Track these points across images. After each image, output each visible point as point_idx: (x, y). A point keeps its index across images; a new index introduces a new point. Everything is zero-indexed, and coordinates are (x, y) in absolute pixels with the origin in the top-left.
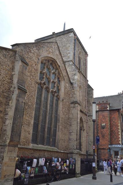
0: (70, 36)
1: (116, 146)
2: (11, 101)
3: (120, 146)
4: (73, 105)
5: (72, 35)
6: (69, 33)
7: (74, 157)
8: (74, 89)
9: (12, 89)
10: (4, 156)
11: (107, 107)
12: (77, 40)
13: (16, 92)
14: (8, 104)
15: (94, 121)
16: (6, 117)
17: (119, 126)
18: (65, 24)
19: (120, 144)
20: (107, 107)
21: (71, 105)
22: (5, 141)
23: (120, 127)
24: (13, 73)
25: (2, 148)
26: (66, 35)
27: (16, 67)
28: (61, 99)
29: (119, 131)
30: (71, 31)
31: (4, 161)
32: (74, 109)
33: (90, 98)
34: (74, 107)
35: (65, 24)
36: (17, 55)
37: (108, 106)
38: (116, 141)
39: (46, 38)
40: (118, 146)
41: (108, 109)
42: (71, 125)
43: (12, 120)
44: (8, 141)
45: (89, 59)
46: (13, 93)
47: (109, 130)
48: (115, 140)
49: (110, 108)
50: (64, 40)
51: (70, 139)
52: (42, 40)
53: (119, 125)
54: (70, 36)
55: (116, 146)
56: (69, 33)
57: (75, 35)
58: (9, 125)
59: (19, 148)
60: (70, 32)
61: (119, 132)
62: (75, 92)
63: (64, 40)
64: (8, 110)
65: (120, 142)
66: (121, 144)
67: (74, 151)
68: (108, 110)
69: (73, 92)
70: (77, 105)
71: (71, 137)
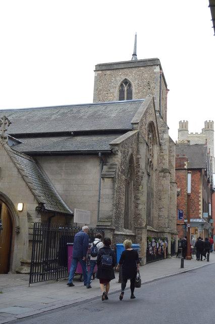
0: (155, 71)
1: (195, 220)
2: (141, 187)
3: (200, 221)
4: (162, 173)
5: (157, 69)
6: (153, 65)
7: (165, 236)
8: (162, 152)
9: (140, 174)
10: (142, 237)
11: (185, 165)
12: (162, 76)
13: (145, 178)
14: (138, 190)
15: (189, 195)
16: (138, 202)
17: (200, 193)
18: (136, 36)
19: (200, 218)
20: (185, 165)
21: (160, 173)
22: (141, 224)
23: (201, 195)
24: (139, 156)
25: (138, 230)
26: (148, 68)
27: (140, 150)
28: (154, 169)
29: (200, 199)
30: (155, 62)
31: (143, 241)
32: (164, 179)
33: (171, 158)
34: (164, 177)
35: (136, 36)
36: (140, 136)
37: (185, 163)
38: (194, 213)
39: (115, 67)
40: (198, 220)
41: (186, 167)
42: (160, 199)
43: (146, 205)
44: (144, 225)
45: (170, 96)
46: (142, 178)
47: (186, 199)
48: (193, 212)
49: (187, 166)
50: (146, 75)
51: (159, 216)
52: (109, 68)
53: (201, 191)
54: (155, 71)
55: (195, 220)
56: (154, 67)
57: (161, 69)
58: (143, 210)
59: (148, 231)
60: (155, 65)
61: (200, 201)
62: (165, 157)
63: (146, 75)
64: (139, 195)
65: (201, 216)
66: (201, 217)
67: (165, 229)
68: (185, 169)
69: (161, 156)
70: (168, 174)
71: (161, 214)
